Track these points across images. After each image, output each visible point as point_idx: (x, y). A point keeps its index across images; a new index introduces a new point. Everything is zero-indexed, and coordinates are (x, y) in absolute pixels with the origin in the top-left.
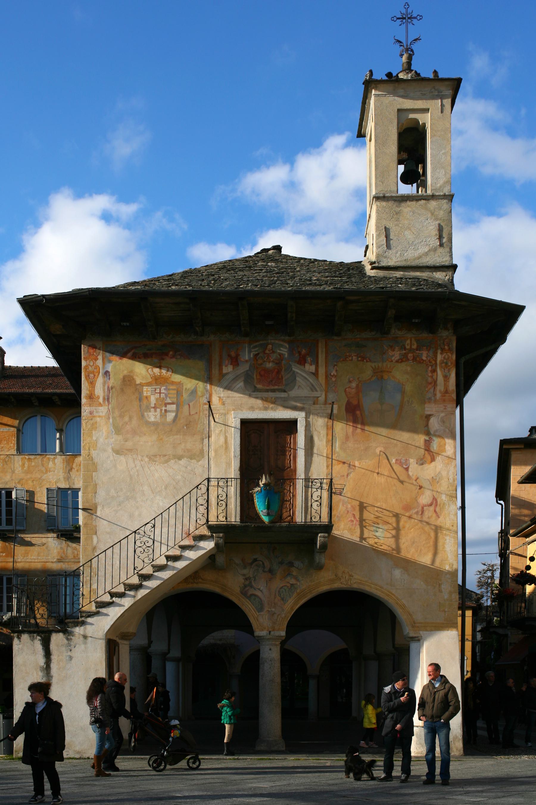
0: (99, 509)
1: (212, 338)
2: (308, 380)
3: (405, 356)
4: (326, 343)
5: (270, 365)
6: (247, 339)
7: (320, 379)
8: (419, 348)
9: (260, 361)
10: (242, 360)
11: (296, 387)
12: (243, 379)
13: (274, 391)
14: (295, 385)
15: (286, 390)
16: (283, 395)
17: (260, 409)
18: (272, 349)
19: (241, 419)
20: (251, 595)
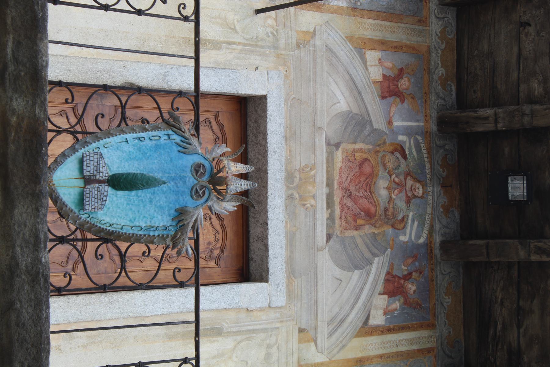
1: (435, 26)
2: (353, 307)
4: (429, 350)
6: (433, 127)
7: (356, 342)
9: (390, 161)
10: (393, 109)
11: (338, 272)
12: (355, 110)
13: (330, 204)
14: (342, 268)
15: (331, 242)
16: (321, 231)
17: (289, 161)
18: (415, 197)
19: (263, 99)
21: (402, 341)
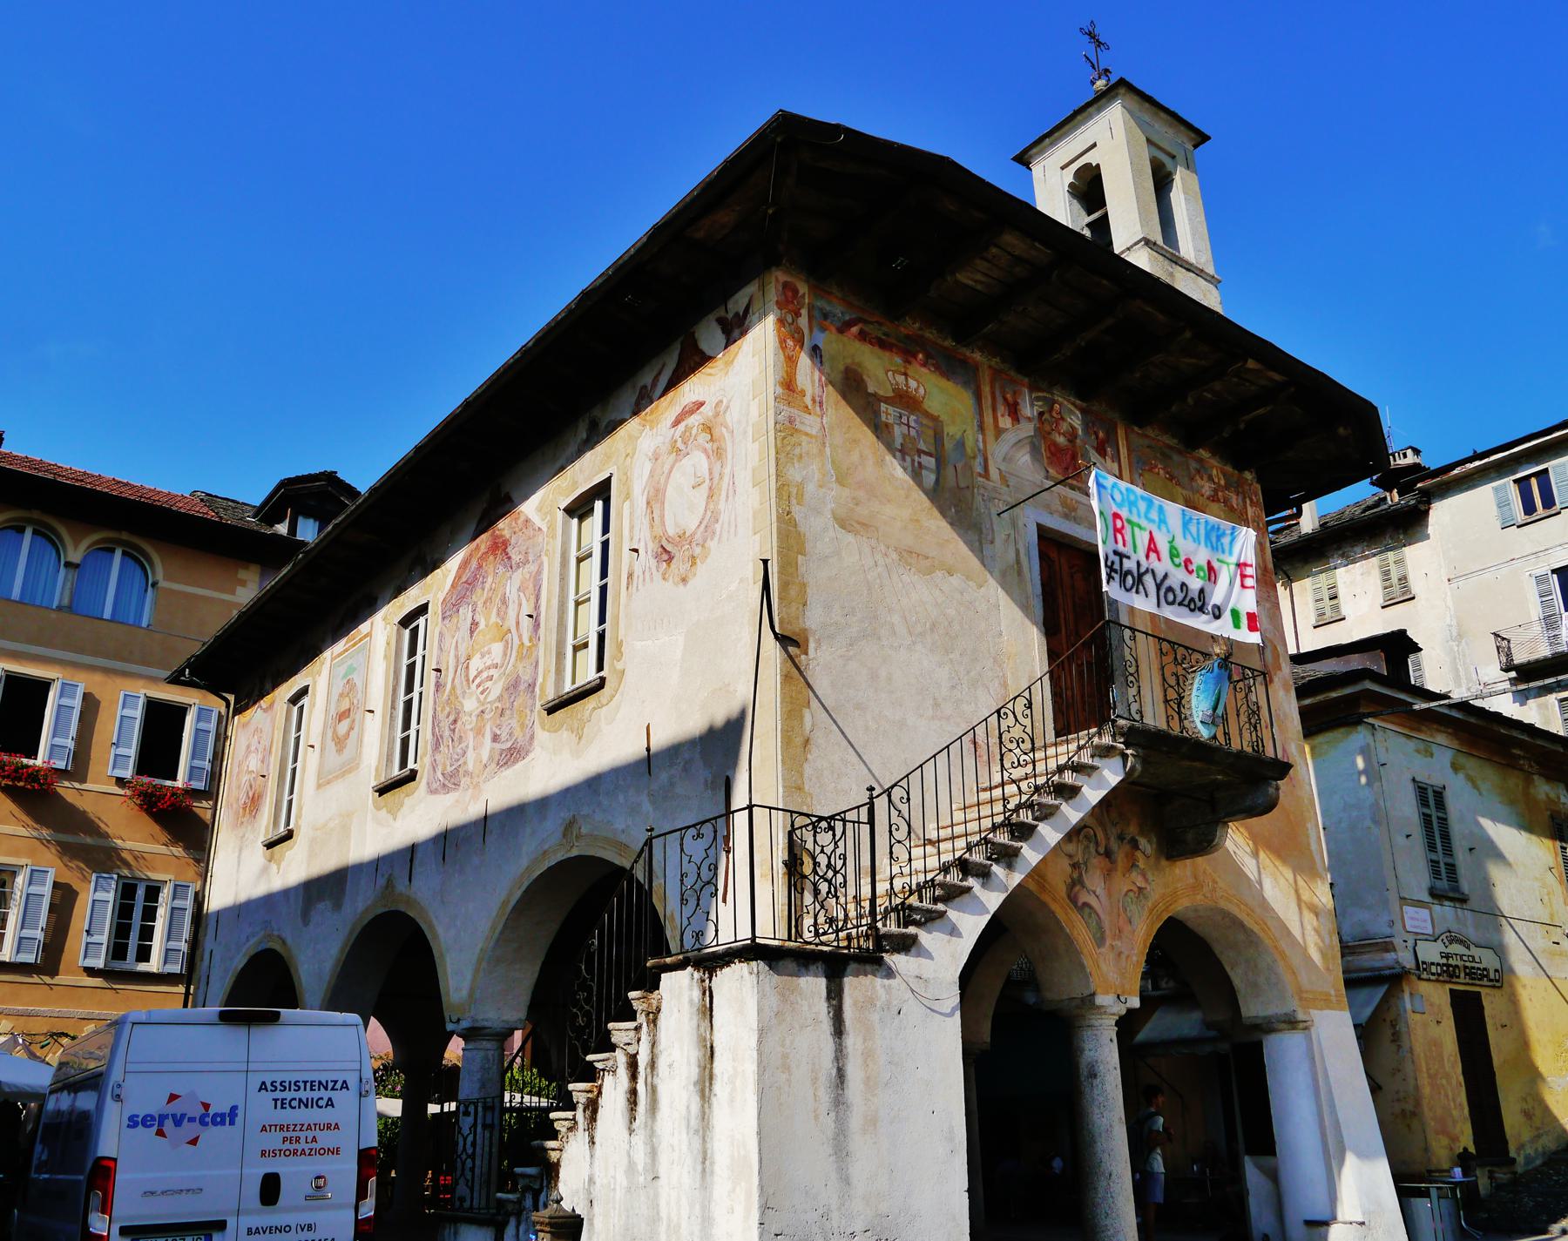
0: (812, 645)
1: (977, 356)
3: (1216, 491)
5: (1061, 440)
8: (1227, 487)
12: (1027, 448)
20: (1086, 904)
21: (1123, 451)
